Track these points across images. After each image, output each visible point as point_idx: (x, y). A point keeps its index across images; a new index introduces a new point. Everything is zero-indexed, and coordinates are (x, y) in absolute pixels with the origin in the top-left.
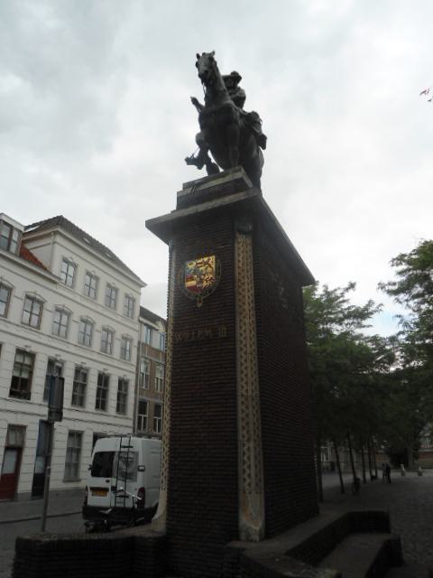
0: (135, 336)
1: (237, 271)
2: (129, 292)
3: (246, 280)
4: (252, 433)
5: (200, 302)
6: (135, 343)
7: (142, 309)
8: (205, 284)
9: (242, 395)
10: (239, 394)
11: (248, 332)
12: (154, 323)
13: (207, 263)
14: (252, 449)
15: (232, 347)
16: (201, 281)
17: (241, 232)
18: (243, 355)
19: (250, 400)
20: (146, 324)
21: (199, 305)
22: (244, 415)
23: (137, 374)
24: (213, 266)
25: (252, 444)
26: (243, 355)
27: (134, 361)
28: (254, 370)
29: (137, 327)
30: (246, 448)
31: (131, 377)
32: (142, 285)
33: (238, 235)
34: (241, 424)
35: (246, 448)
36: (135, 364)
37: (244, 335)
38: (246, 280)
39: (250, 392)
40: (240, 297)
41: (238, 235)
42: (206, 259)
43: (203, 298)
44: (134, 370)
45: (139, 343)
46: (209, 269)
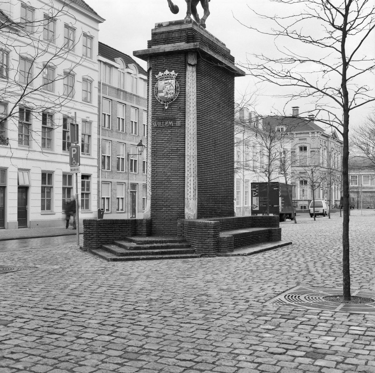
0: (96, 77)
1: (187, 88)
2: (87, 30)
3: (192, 94)
4: (192, 173)
5: (166, 106)
6: (95, 84)
7: (100, 44)
8: (169, 96)
9: (188, 155)
10: (186, 154)
11: (192, 122)
12: (114, 61)
13: (170, 84)
14: (192, 180)
15: (184, 131)
17: (190, 65)
18: (189, 135)
19: (192, 157)
20: (105, 63)
21: (166, 108)
22: (189, 165)
23: (99, 116)
24: (174, 85)
25: (192, 179)
26: (189, 135)
27: (95, 102)
28: (194, 143)
29: (97, 66)
30: (189, 180)
31: (94, 119)
32: (98, 20)
33: (188, 67)
34: (186, 169)
35: (189, 180)
36: (97, 105)
38: (192, 94)
39: (192, 154)
40: (189, 104)
41: (188, 67)
42: (170, 81)
44: (96, 111)
45: (99, 83)
46: (172, 87)
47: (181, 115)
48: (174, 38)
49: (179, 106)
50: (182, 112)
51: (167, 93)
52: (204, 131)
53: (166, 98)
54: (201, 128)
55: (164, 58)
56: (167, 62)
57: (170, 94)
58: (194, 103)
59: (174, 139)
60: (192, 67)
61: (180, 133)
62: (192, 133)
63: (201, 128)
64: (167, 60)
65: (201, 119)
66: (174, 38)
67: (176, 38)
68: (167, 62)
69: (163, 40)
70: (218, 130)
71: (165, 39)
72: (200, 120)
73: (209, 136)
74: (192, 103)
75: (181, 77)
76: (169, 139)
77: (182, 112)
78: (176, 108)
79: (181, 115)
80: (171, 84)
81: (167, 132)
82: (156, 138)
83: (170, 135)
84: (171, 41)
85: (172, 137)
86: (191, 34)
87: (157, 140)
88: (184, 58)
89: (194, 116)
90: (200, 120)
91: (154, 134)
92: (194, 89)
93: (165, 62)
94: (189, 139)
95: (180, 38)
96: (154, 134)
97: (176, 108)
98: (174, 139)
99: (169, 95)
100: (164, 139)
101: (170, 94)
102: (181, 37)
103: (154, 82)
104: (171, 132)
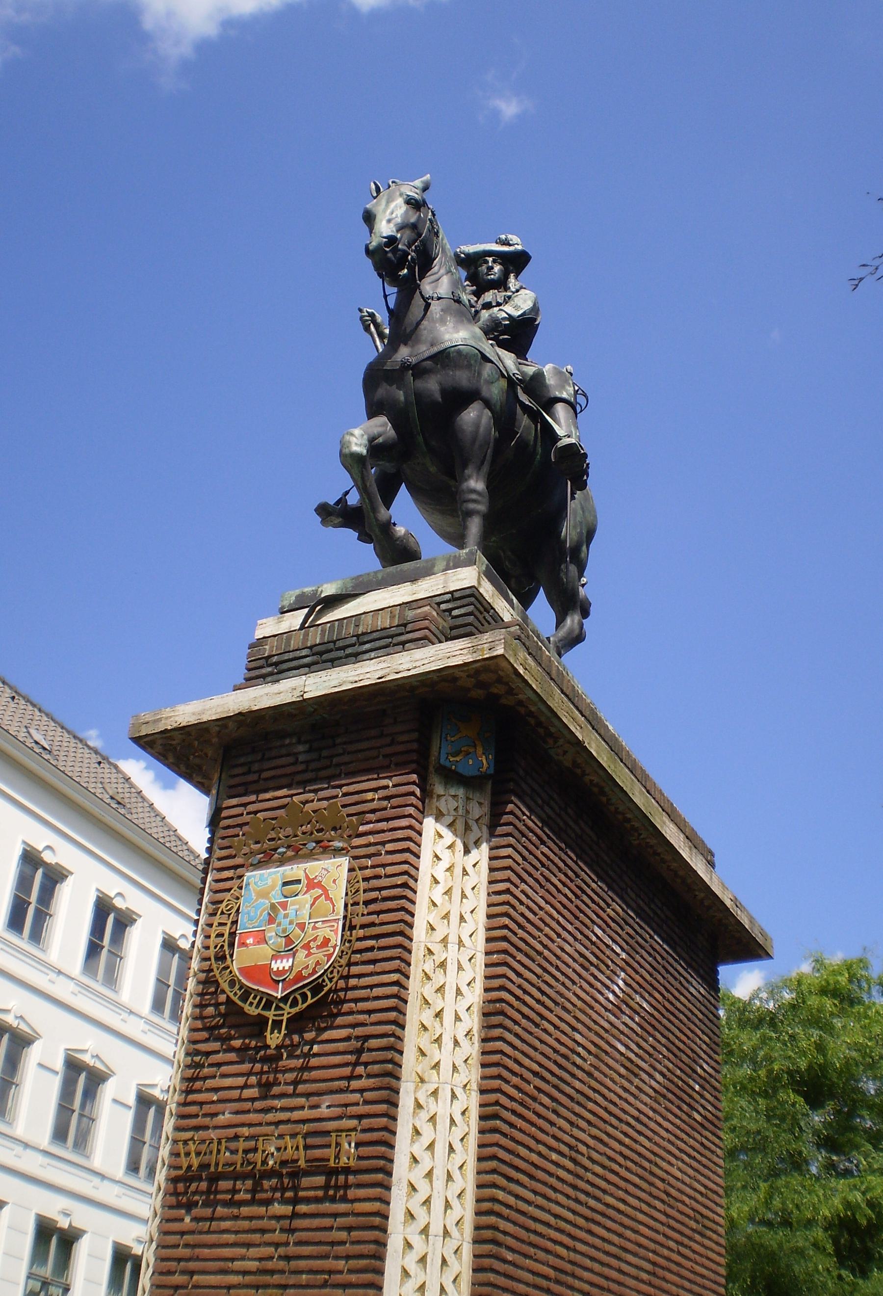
5: (277, 1024)
16: (290, 949)
17: (452, 777)
18: (417, 1240)
26: (417, 1240)
33: (439, 789)
37: (426, 1163)
43: (288, 1011)
47: (368, 1095)
48: (366, 638)
49: (359, 1031)
50: (376, 1068)
51: (289, 940)
52: (532, 1225)
53: (279, 972)
54: (501, 1195)
55: (301, 748)
56: (313, 766)
57: (307, 947)
58: (463, 1015)
59: (302, 1264)
60: (461, 792)
61: (350, 1220)
62: (436, 1229)
63: (501, 1195)
64: (314, 755)
65: (505, 1128)
66: (366, 638)
67: (375, 635)
68: (313, 766)
69: (304, 652)
70: (628, 1233)
71: (315, 649)
72: (504, 1141)
73: (568, 1267)
74: (449, 1017)
75: (389, 847)
76: (269, 1265)
77: (376, 1068)
78: (341, 1046)
79: (368, 1095)
80: (319, 885)
81: (262, 1210)
82: (187, 1252)
83: (277, 1236)
84: (349, 651)
85: (292, 1250)
86: (471, 619)
87: (192, 1265)
88: (415, 735)
89: (458, 1107)
90: (504, 1141)
91: (175, 1226)
92: (468, 928)
93: (301, 767)
94: (413, 1268)
95: (401, 629)
96: (175, 1226)
97: (341, 1046)
98: (302, 1264)
99: (301, 954)
100: (238, 1265)
101: (307, 947)
102: (410, 627)
103: (227, 885)
104: (287, 1209)
